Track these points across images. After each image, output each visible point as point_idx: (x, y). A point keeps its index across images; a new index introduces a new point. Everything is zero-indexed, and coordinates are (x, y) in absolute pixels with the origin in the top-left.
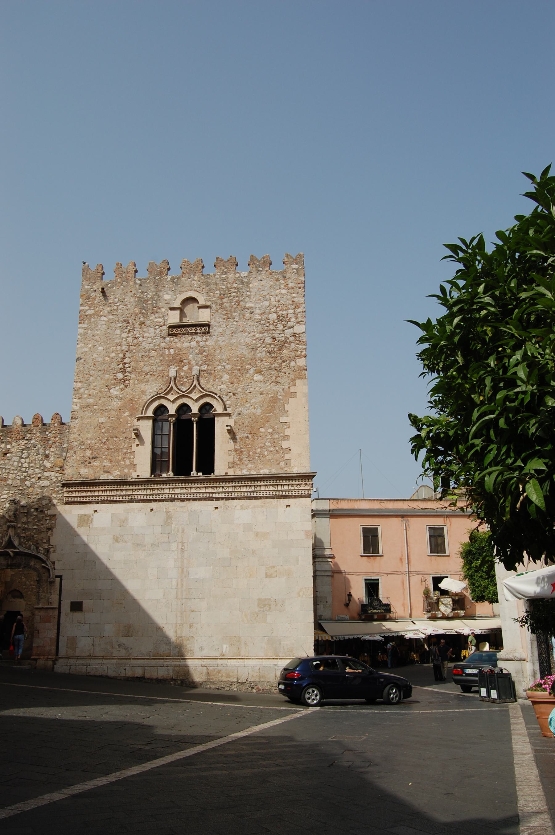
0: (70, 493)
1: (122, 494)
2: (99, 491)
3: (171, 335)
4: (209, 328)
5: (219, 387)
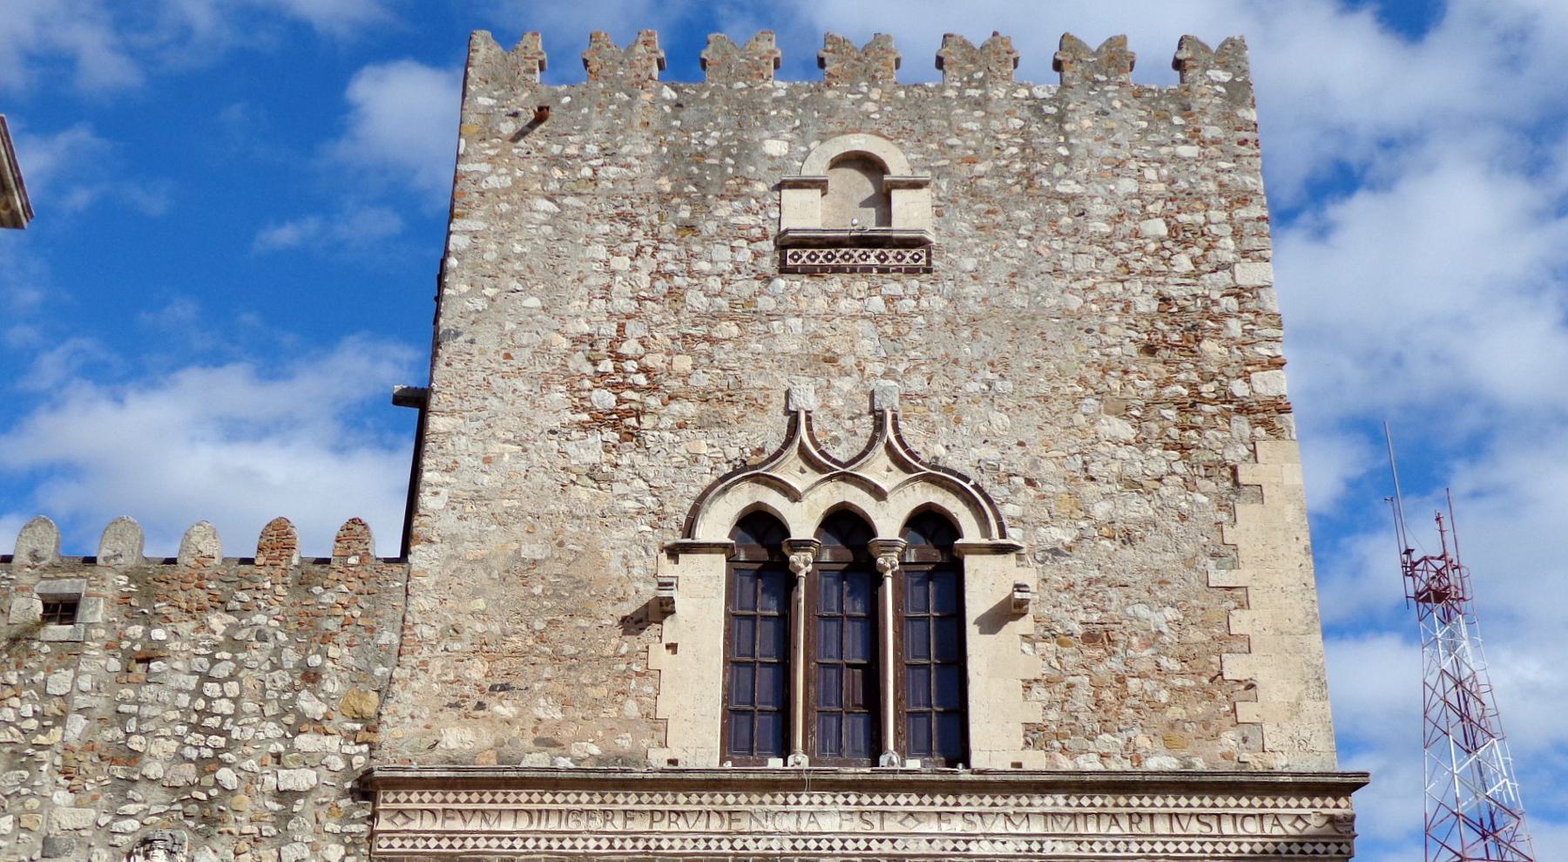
0: (400, 820)
1: (609, 828)
3: (793, 271)
4: (929, 254)
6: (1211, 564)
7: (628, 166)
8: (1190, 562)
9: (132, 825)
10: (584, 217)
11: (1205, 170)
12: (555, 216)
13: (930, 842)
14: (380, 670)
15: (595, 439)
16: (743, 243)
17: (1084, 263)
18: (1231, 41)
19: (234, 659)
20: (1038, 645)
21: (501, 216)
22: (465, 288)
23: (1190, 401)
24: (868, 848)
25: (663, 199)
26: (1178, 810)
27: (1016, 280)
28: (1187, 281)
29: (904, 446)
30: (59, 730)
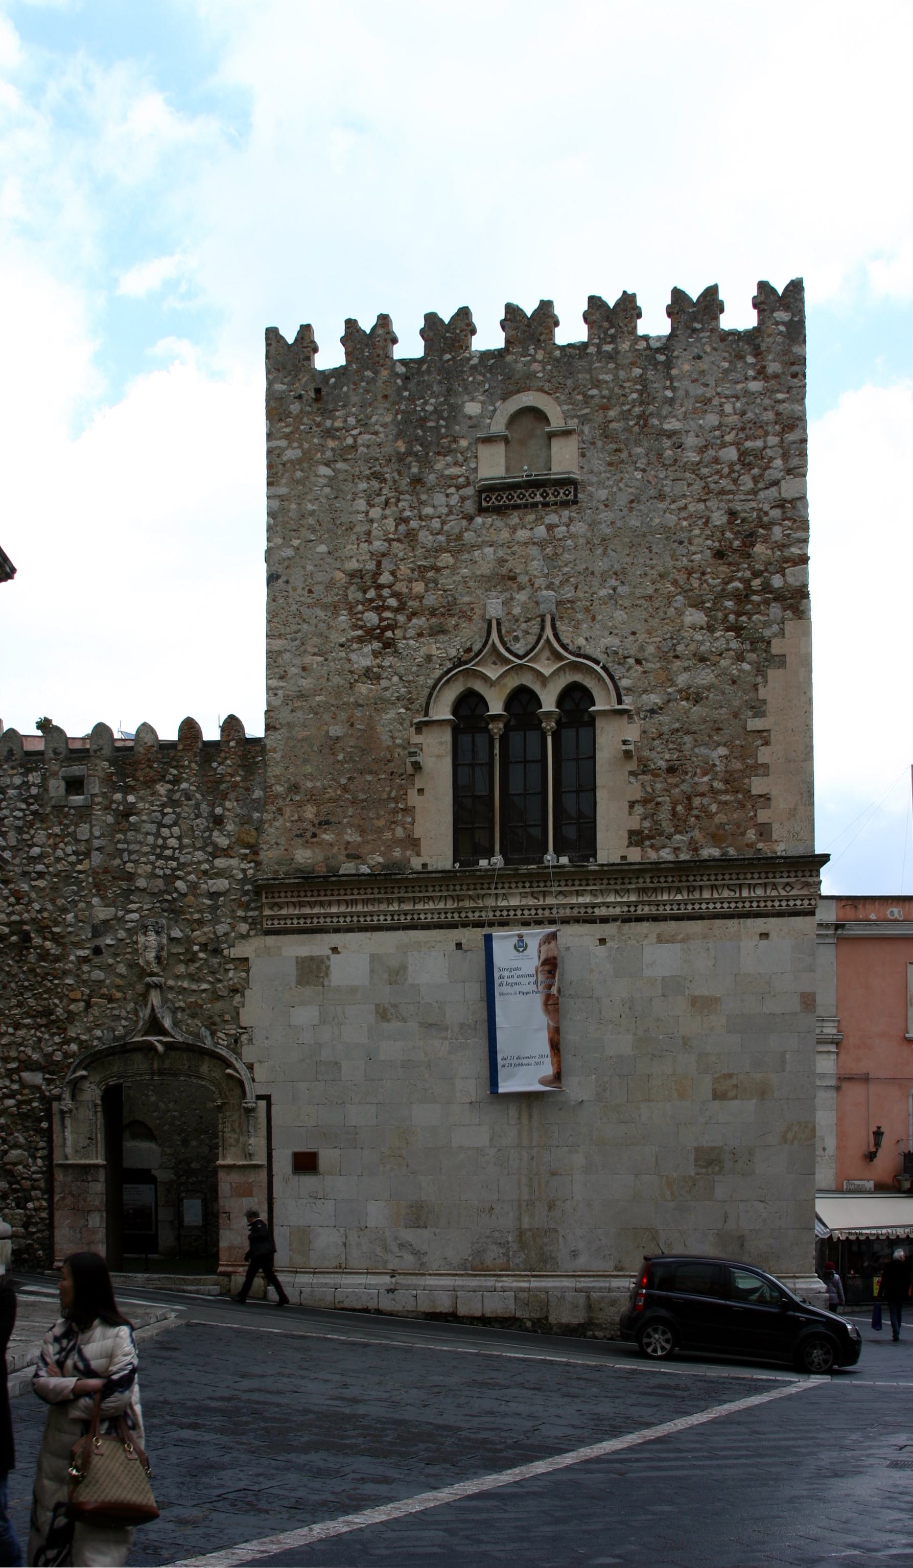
0: (276, 909)
1: (391, 908)
2: (339, 903)
4: (576, 490)
7: (376, 433)
10: (350, 478)
11: (767, 402)
12: (331, 479)
13: (572, 908)
14: (256, 815)
15: (367, 649)
16: (452, 490)
19: (174, 812)
20: (640, 777)
21: (298, 482)
23: (744, 593)
25: (401, 458)
27: (634, 505)
28: (750, 497)
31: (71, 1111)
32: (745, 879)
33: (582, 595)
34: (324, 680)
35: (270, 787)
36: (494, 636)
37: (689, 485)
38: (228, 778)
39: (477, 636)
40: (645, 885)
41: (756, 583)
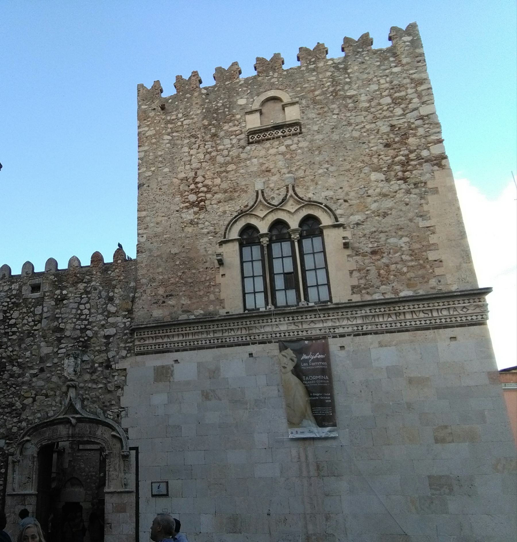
0: (142, 341)
1: (209, 336)
3: (252, 143)
4: (300, 128)
5: (324, 194)
6: (420, 219)
7: (193, 119)
8: (411, 220)
9: (64, 350)
11: (404, 75)
12: (170, 140)
13: (320, 330)
15: (191, 211)
17: (361, 119)
18: (410, 25)
20: (354, 257)
21: (154, 144)
22: (145, 169)
23: (406, 161)
24: (298, 334)
25: (205, 127)
26: (414, 310)
28: (402, 117)
29: (297, 196)
30: (40, 324)
31: (19, 461)
32: (434, 306)
33: (308, 173)
34: (168, 228)
35: (139, 280)
36: (260, 197)
37: (365, 117)
38: (117, 278)
39: (251, 199)
40: (366, 314)
41: (412, 156)
